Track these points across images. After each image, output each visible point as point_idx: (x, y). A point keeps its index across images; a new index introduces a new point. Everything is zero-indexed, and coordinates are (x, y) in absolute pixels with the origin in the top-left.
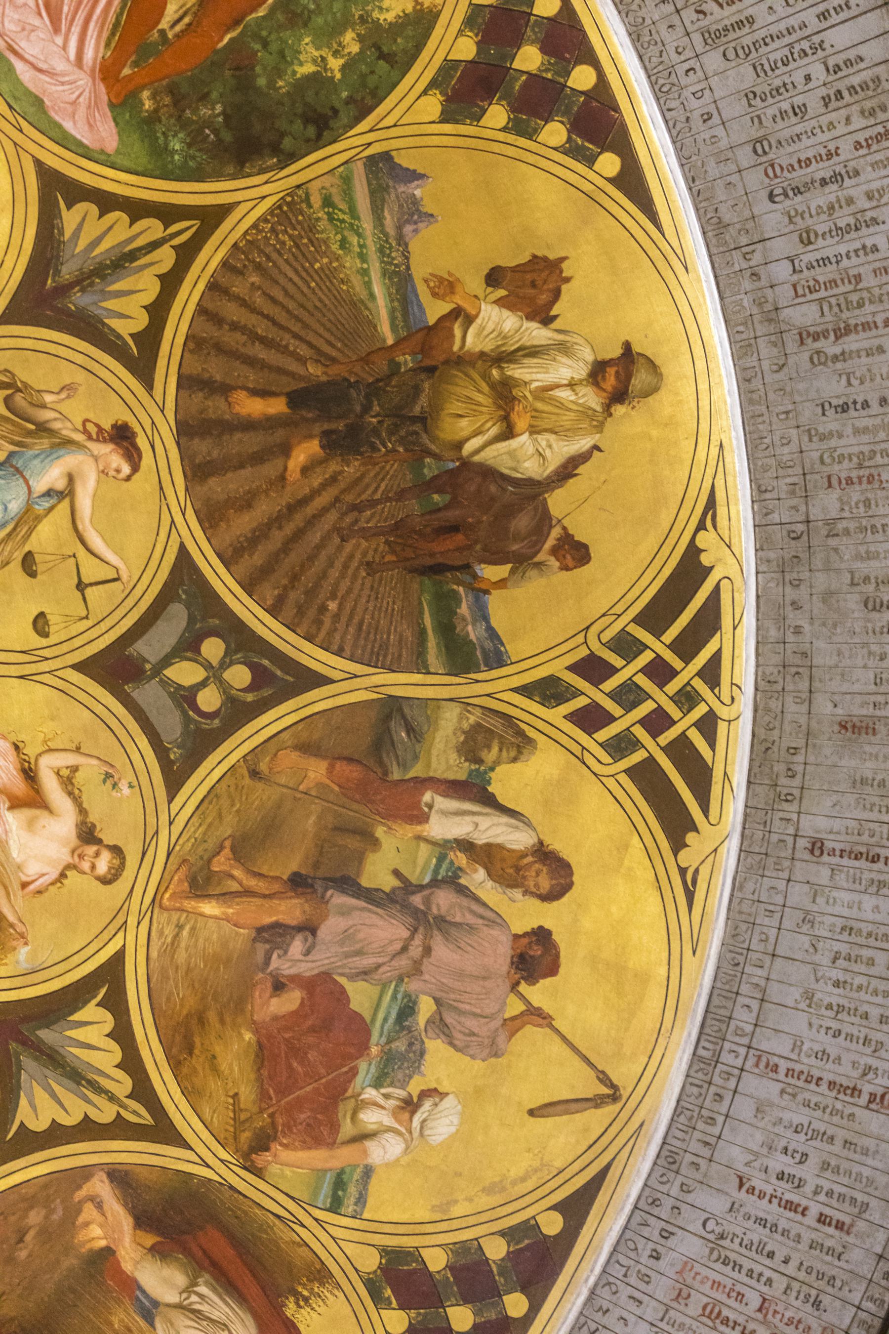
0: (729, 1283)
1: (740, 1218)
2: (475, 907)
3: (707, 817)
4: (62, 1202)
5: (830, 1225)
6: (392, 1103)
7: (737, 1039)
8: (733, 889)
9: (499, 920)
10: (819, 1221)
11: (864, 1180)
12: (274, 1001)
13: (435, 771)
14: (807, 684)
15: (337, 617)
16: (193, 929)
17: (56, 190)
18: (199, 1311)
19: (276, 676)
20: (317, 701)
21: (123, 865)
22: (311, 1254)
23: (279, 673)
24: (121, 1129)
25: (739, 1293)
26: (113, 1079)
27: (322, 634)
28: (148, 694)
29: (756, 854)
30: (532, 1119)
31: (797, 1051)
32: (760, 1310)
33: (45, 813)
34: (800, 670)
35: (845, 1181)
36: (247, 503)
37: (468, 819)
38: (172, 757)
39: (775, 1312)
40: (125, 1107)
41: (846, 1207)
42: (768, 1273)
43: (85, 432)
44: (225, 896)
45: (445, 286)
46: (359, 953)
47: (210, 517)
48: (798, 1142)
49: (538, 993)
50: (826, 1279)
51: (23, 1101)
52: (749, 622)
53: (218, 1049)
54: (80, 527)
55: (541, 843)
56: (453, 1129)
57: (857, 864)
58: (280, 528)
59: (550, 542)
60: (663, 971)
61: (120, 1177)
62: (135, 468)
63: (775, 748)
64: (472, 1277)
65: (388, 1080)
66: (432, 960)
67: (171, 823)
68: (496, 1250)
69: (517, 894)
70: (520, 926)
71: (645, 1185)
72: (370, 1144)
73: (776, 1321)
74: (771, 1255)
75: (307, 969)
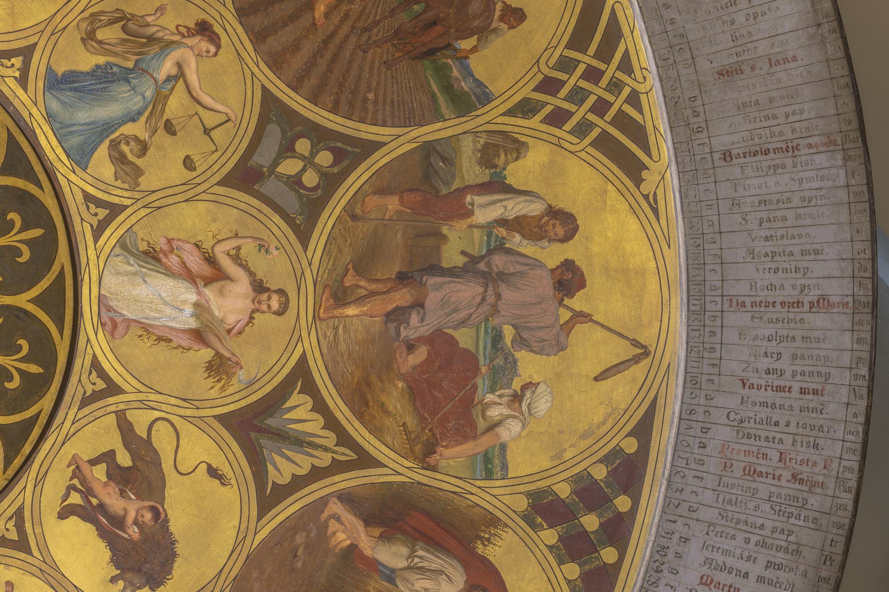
0: (755, 450)
1: (750, 406)
2: (520, 259)
3: (651, 158)
4: (314, 524)
5: (809, 393)
6: (505, 399)
7: (713, 293)
8: (681, 198)
9: (539, 264)
10: (801, 393)
11: (822, 358)
12: (410, 357)
13: (469, 180)
14: (689, 54)
15: (375, 102)
16: (345, 327)
18: (422, 567)
19: (347, 151)
20: (380, 159)
21: (287, 300)
22: (482, 510)
23: (349, 149)
24: (337, 467)
25: (763, 454)
26: (323, 437)
27: (370, 116)
28: (270, 187)
29: (689, 173)
30: (598, 383)
31: (754, 289)
32: (780, 460)
33: (229, 282)
34: (682, 46)
35: (810, 362)
36: (296, 47)
37: (498, 205)
38: (298, 222)
39: (791, 459)
40: (336, 453)
41: (816, 379)
42: (778, 436)
43: (179, 33)
44: (359, 301)
46: (455, 311)
47: (276, 63)
48: (772, 347)
49: (577, 303)
50: (817, 428)
51: (270, 468)
52: (640, 25)
53: (384, 398)
54: (195, 94)
55: (550, 206)
56: (549, 404)
57: (756, 159)
58: (322, 57)
59: (497, 14)
60: (652, 264)
61: (346, 498)
62: (218, 47)
63: (681, 101)
64: (590, 494)
65: (499, 386)
66: (503, 301)
67: (310, 265)
68: (600, 473)
69: (545, 243)
70: (552, 263)
71: (682, 403)
72: (499, 430)
73: (793, 464)
74: (777, 424)
75: (425, 330)
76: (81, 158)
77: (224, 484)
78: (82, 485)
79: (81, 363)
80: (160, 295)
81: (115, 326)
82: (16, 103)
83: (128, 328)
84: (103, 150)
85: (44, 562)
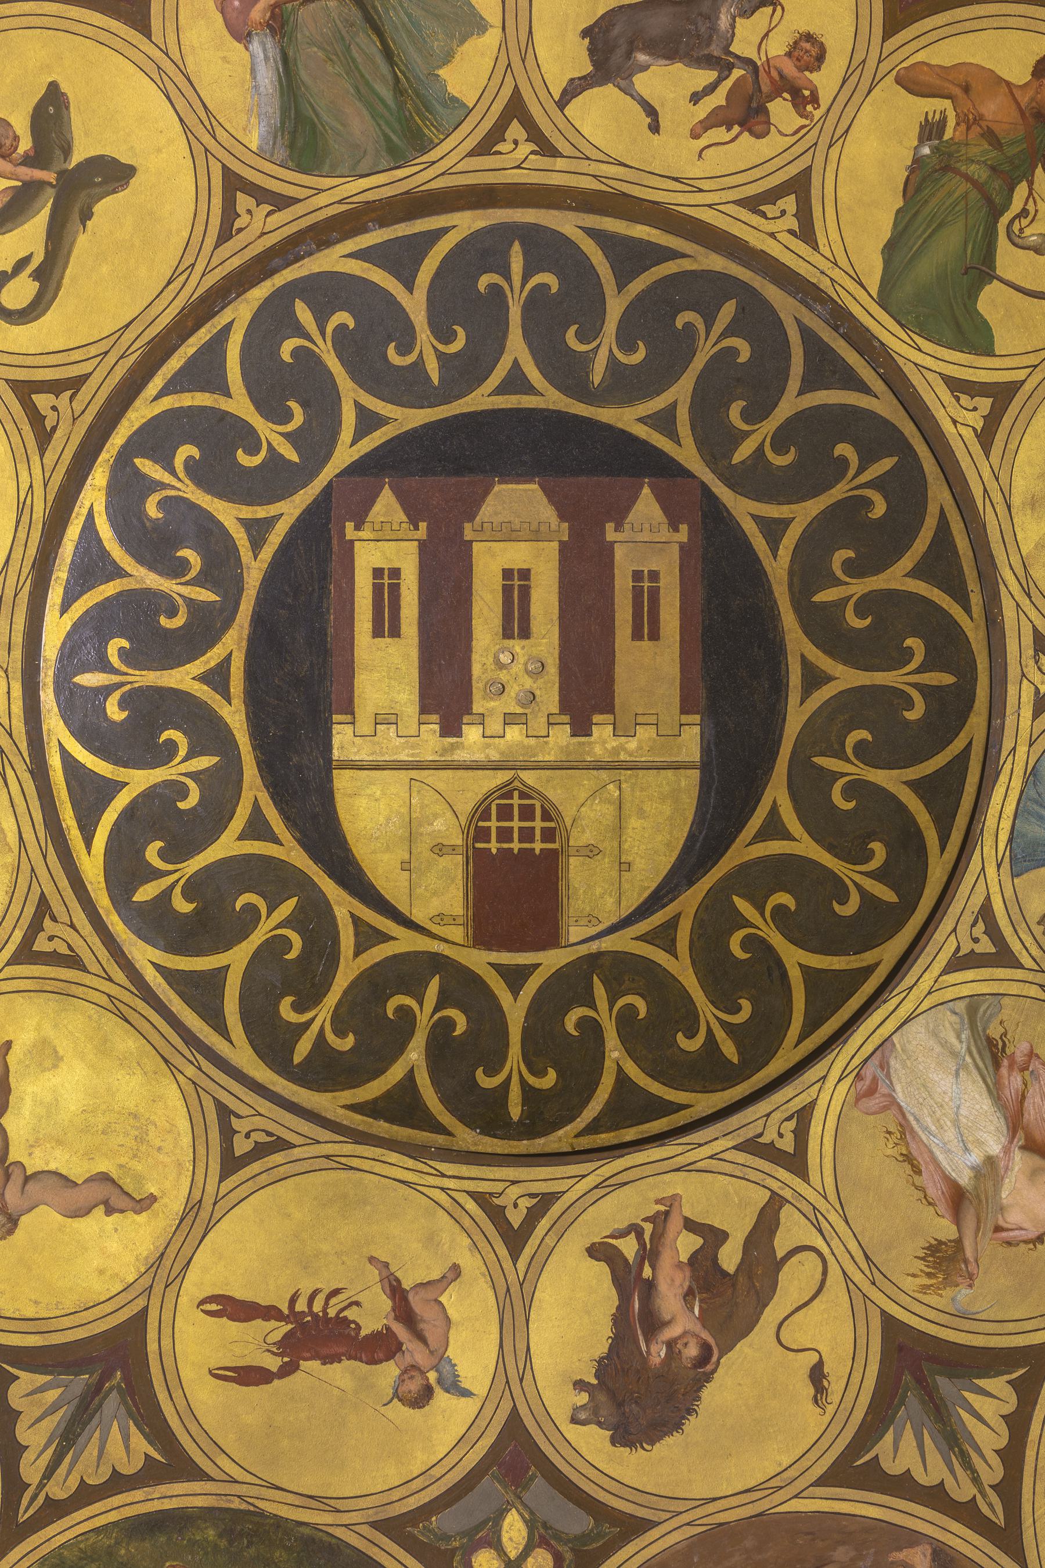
24: (967, 1513)
26: (986, 1462)
40: (984, 1495)
51: (889, 1437)
76: (1024, 857)
77: (816, 1402)
78: (651, 1240)
79: (789, 1098)
80: (958, 1107)
81: (871, 1091)
82: (1010, 721)
83: (885, 1108)
85: (521, 1285)
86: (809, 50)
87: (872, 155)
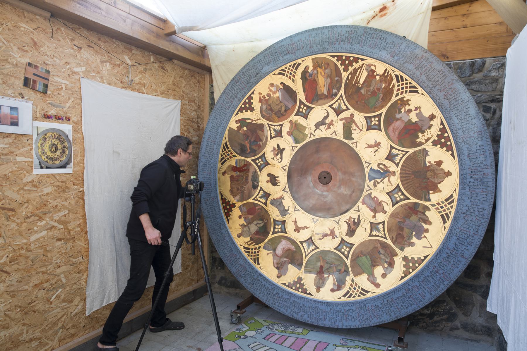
17: (392, 148)
45: (429, 162)
47: (401, 181)
76: (370, 181)
84: (373, 181)
86: (332, 121)
87: (339, 127)
